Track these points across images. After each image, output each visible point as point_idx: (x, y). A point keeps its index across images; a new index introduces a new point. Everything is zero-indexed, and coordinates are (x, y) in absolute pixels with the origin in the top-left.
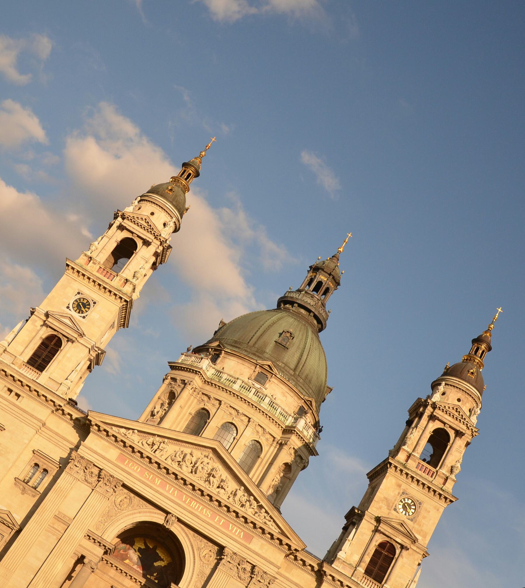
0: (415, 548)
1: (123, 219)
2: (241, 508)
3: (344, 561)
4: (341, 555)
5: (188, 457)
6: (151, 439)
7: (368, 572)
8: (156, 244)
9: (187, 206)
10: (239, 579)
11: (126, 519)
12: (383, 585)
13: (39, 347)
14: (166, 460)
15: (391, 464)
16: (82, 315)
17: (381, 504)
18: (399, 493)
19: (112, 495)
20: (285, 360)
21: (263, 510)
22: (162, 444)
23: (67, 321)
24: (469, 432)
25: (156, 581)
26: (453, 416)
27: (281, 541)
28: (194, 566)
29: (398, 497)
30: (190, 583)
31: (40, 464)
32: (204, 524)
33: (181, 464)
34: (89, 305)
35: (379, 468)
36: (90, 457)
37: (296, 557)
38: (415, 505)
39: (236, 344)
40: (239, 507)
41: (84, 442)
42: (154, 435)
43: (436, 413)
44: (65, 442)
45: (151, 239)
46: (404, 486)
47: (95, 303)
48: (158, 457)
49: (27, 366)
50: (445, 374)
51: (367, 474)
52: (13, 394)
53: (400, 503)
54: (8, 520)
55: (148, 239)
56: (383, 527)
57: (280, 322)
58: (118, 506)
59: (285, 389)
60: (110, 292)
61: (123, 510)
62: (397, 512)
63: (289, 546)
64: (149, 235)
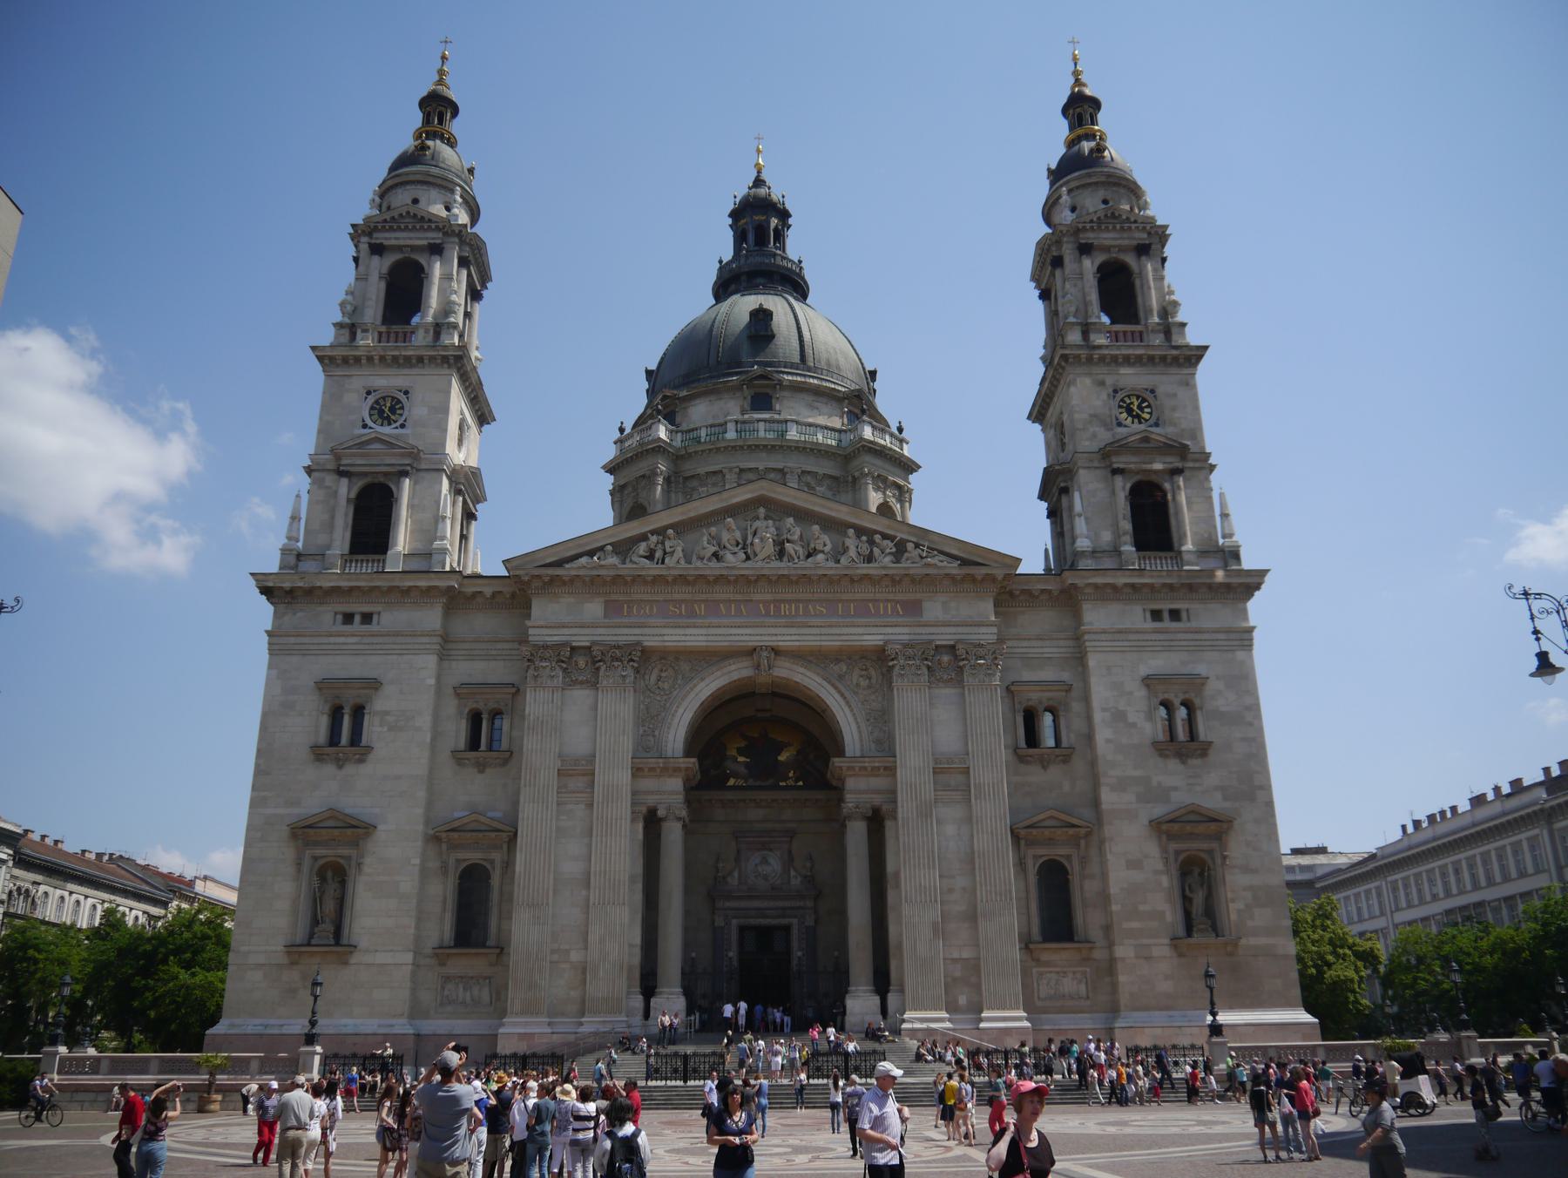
0: (1190, 464)
1: (370, 235)
2: (871, 565)
3: (1094, 552)
4: (1083, 543)
5: (725, 537)
6: (642, 548)
7: (1140, 545)
8: (453, 243)
9: (467, 166)
10: (941, 684)
11: (685, 704)
12: (1180, 552)
13: (355, 519)
14: (689, 562)
15: (1065, 357)
16: (398, 424)
17: (1091, 430)
18: (1109, 395)
19: (635, 678)
20: (781, 355)
21: (910, 546)
22: (668, 544)
23: (377, 446)
24: (1155, 240)
25: (801, 783)
26: (1114, 228)
27: (973, 579)
28: (852, 711)
29: (1111, 402)
30: (861, 740)
31: (481, 706)
32: (824, 631)
33: (721, 553)
34: (399, 402)
35: (1046, 385)
36: (556, 638)
37: (1011, 594)
38: (1144, 400)
39: (688, 379)
40: (866, 565)
41: (528, 616)
42: (643, 537)
43: (1083, 239)
44: (499, 646)
45: (438, 238)
46: (1109, 380)
47: (406, 393)
48: (675, 563)
49: (355, 557)
50: (1052, 184)
51: (1028, 418)
52: (357, 618)
53: (1120, 410)
54: (483, 828)
55: (432, 241)
56: (1119, 462)
57: (736, 310)
58: (657, 692)
59: (809, 398)
60: (420, 360)
61: (671, 693)
62: (1125, 426)
63: (991, 579)
64: (430, 235)
